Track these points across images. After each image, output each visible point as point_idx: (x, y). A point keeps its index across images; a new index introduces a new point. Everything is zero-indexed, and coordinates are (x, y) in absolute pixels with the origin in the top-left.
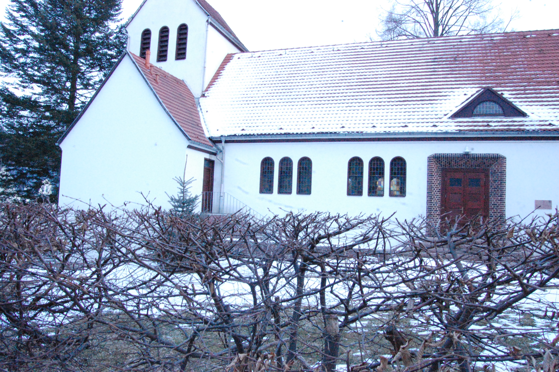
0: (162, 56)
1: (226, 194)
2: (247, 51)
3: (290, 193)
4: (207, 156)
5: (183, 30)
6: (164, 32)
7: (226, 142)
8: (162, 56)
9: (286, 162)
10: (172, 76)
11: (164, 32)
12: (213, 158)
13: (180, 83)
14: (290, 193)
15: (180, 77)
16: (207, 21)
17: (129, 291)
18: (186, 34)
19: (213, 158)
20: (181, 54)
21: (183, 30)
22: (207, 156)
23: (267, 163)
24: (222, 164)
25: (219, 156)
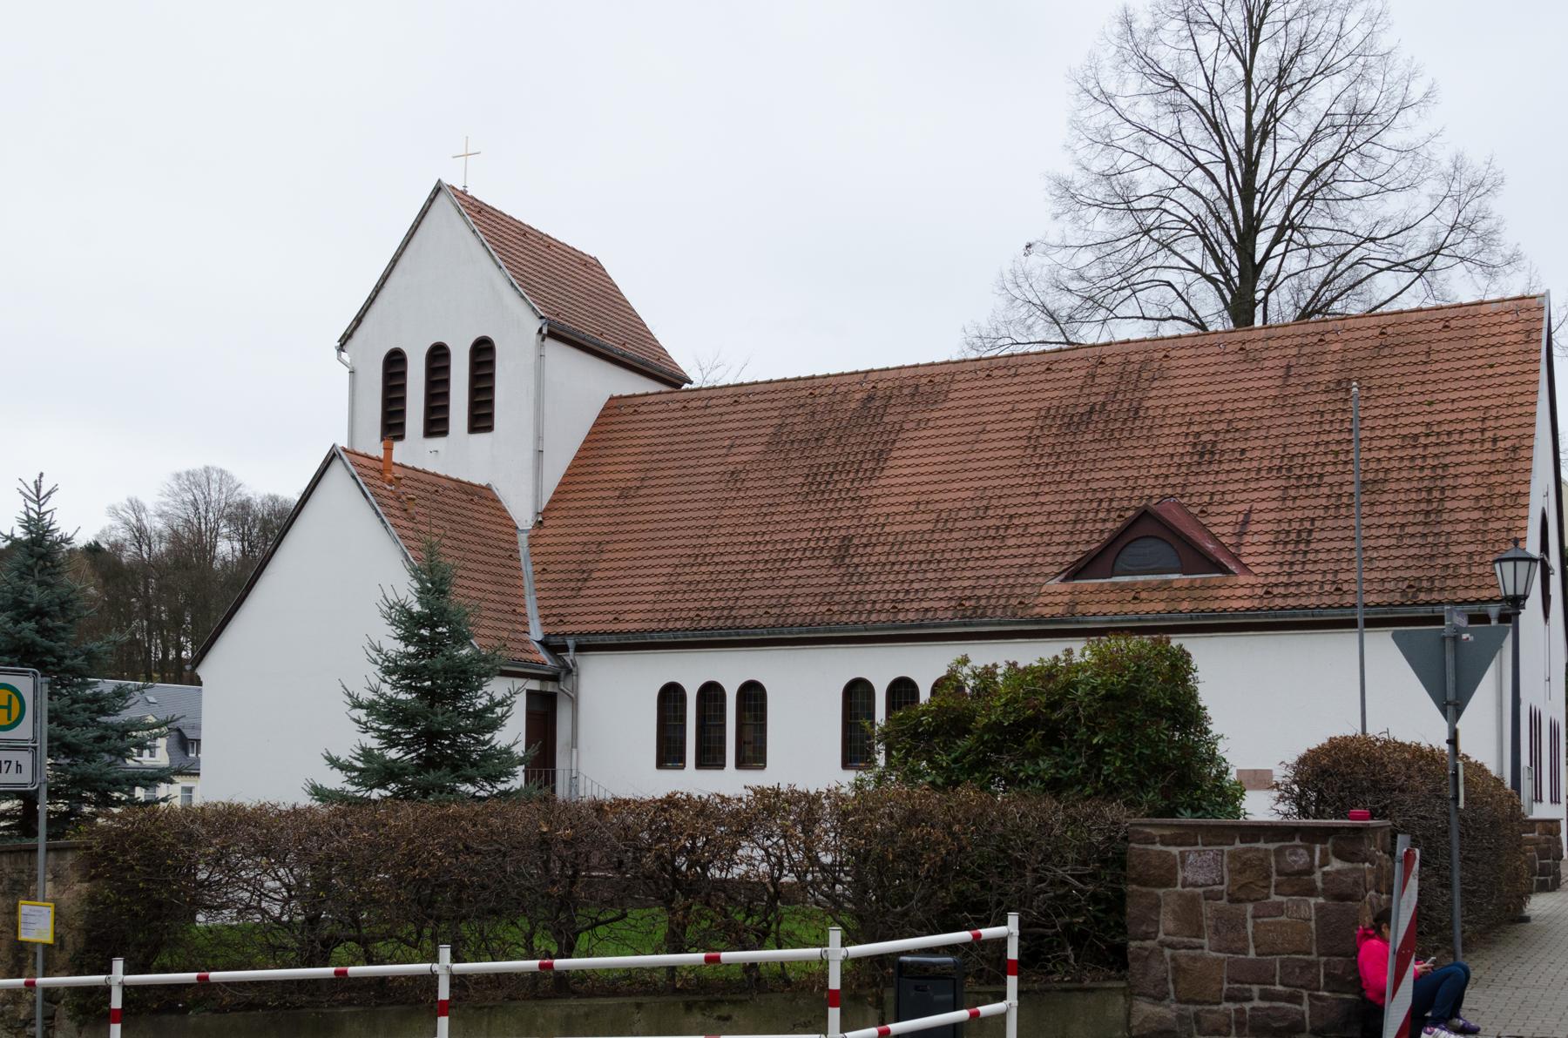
0: (436, 425)
1: (581, 778)
2: (270, 530)
3: (722, 766)
4: (534, 685)
5: (483, 352)
6: (438, 356)
7: (580, 648)
8: (436, 425)
9: (711, 693)
10: (458, 481)
11: (438, 356)
12: (550, 687)
13: (481, 496)
14: (722, 766)
15: (478, 479)
16: (540, 331)
17: (1255, 127)
18: (491, 363)
19: (550, 687)
20: (481, 420)
21: (483, 352)
22: (534, 685)
23: (671, 696)
24: (574, 701)
25: (565, 686)
